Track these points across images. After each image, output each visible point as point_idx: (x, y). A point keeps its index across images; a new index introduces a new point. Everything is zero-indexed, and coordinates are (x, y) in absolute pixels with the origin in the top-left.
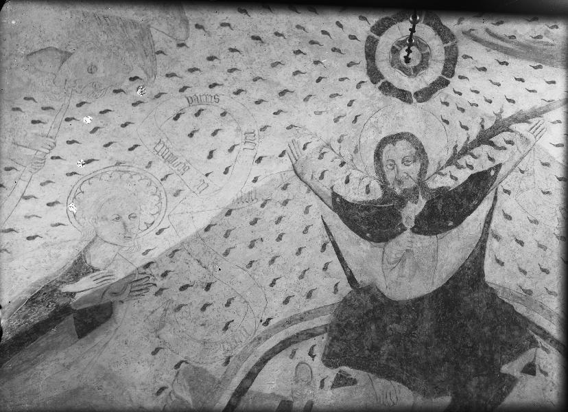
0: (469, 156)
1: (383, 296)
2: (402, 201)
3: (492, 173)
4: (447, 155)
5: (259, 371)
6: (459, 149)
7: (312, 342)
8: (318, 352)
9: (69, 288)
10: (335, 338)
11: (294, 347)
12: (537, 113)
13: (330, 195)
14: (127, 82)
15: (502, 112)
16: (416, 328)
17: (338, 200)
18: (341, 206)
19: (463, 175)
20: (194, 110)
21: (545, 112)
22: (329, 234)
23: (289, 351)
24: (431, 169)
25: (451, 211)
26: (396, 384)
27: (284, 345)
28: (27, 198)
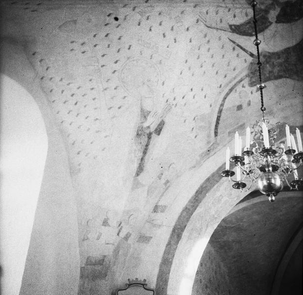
1: (269, 53)
2: (267, 11)
5: (224, 102)
7: (243, 82)
8: (246, 85)
9: (146, 125)
10: (251, 78)
11: (235, 89)
13: (228, 27)
14: (108, 18)
16: (288, 59)
17: (233, 27)
18: (237, 29)
20: (145, 18)
22: (234, 42)
23: (234, 91)
26: (284, 79)
27: (231, 90)
28: (106, 89)
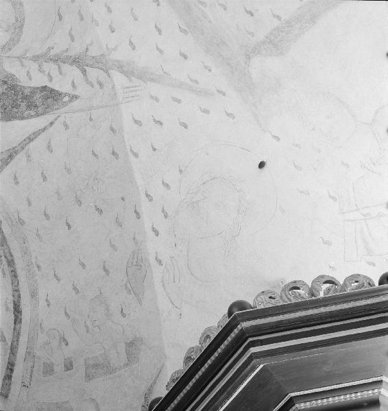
0: (57, 67)
3: (66, 99)
4: (38, 49)
6: (52, 53)
12: (144, 76)
15: (115, 49)
19: (38, 81)
21: (152, 80)
24: (17, 51)
25: (6, 103)
